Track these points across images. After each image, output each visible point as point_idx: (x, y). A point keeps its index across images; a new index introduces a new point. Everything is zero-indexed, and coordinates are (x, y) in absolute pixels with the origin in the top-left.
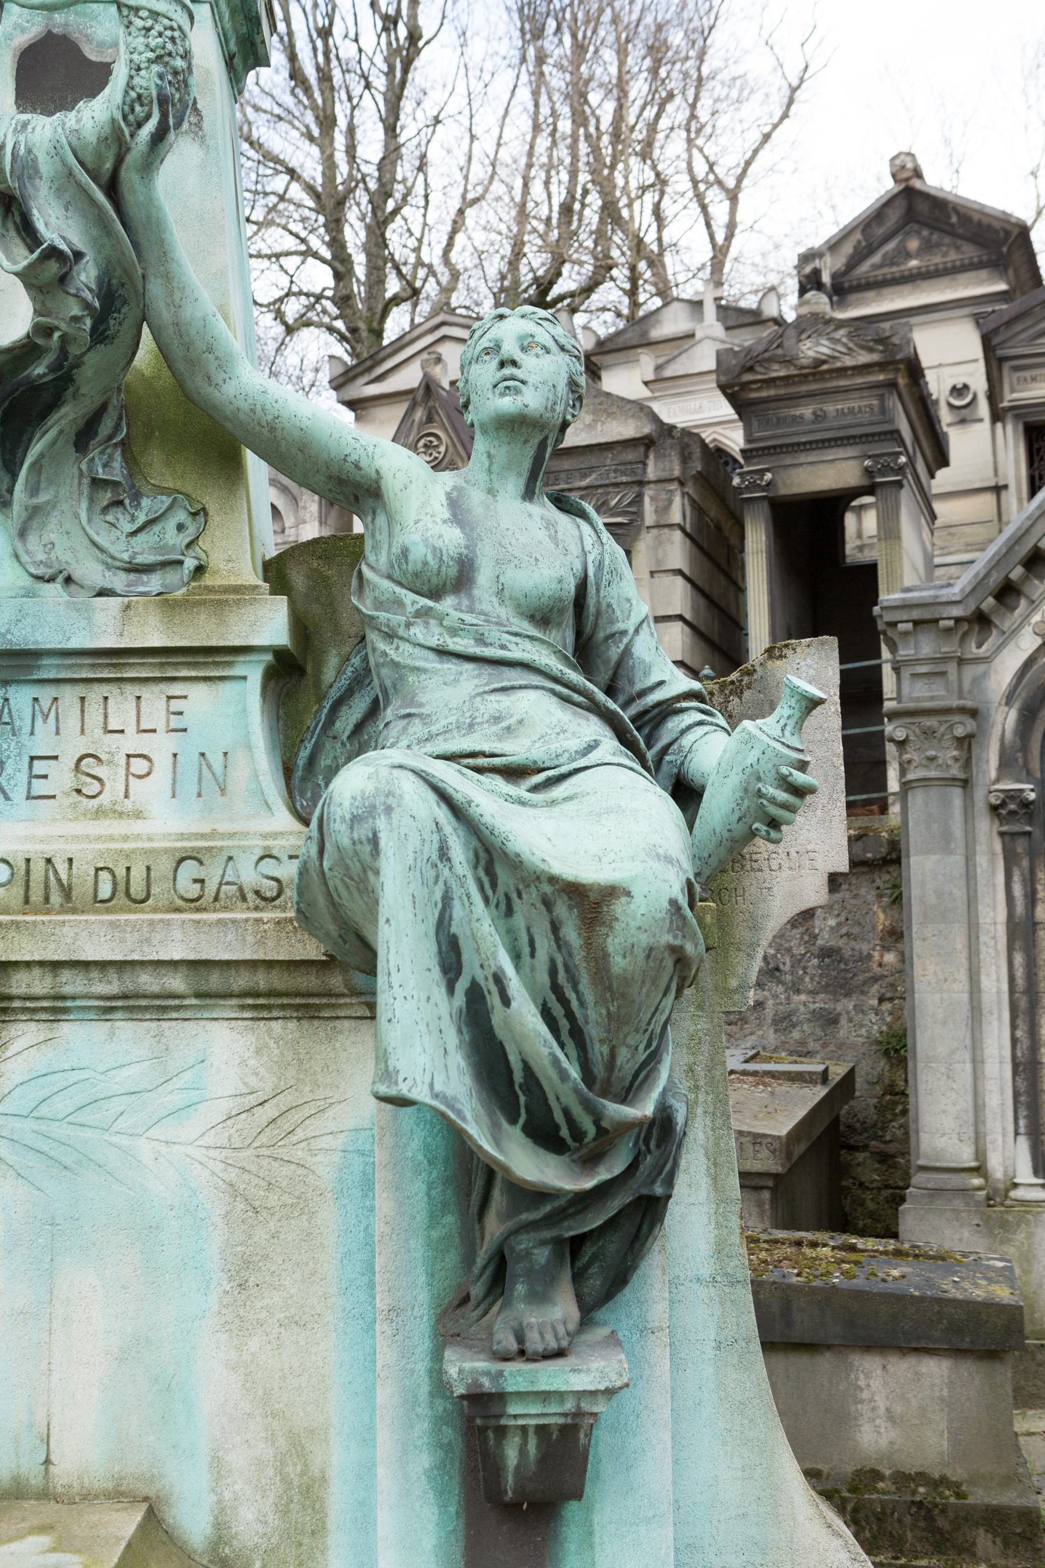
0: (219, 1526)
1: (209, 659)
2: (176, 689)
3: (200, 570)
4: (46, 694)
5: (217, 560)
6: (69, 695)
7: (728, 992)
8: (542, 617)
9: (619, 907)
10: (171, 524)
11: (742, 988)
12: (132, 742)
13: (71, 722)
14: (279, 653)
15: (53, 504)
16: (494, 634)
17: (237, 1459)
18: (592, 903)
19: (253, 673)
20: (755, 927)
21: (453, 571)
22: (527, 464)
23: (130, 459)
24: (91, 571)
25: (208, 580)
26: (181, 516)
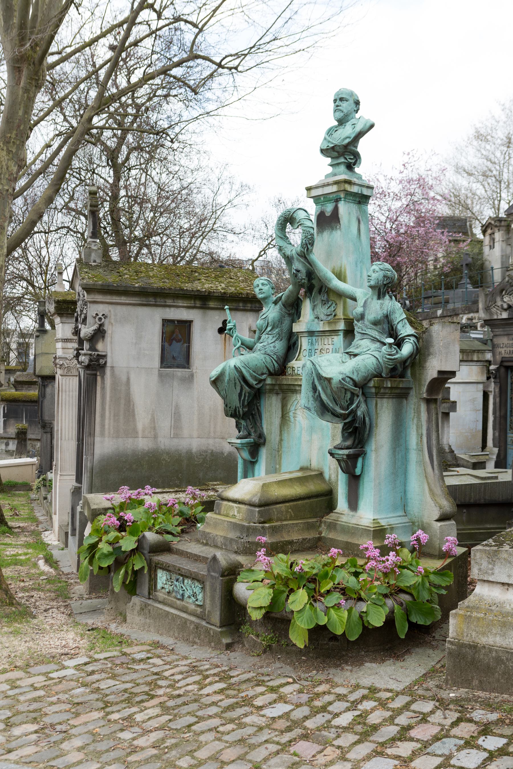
0: (330, 477)
1: (335, 332)
2: (333, 337)
3: (335, 315)
4: (317, 338)
5: (338, 314)
6: (320, 338)
7: (420, 394)
8: (376, 323)
9: (332, 381)
10: (332, 306)
11: (423, 393)
12: (327, 347)
13: (320, 343)
14: (344, 330)
15: (317, 304)
16: (364, 328)
17: (332, 467)
18: (329, 380)
19: (341, 334)
20: (425, 381)
21: (360, 317)
22: (377, 293)
23: (328, 295)
24: (322, 316)
25: (337, 317)
26: (334, 305)
